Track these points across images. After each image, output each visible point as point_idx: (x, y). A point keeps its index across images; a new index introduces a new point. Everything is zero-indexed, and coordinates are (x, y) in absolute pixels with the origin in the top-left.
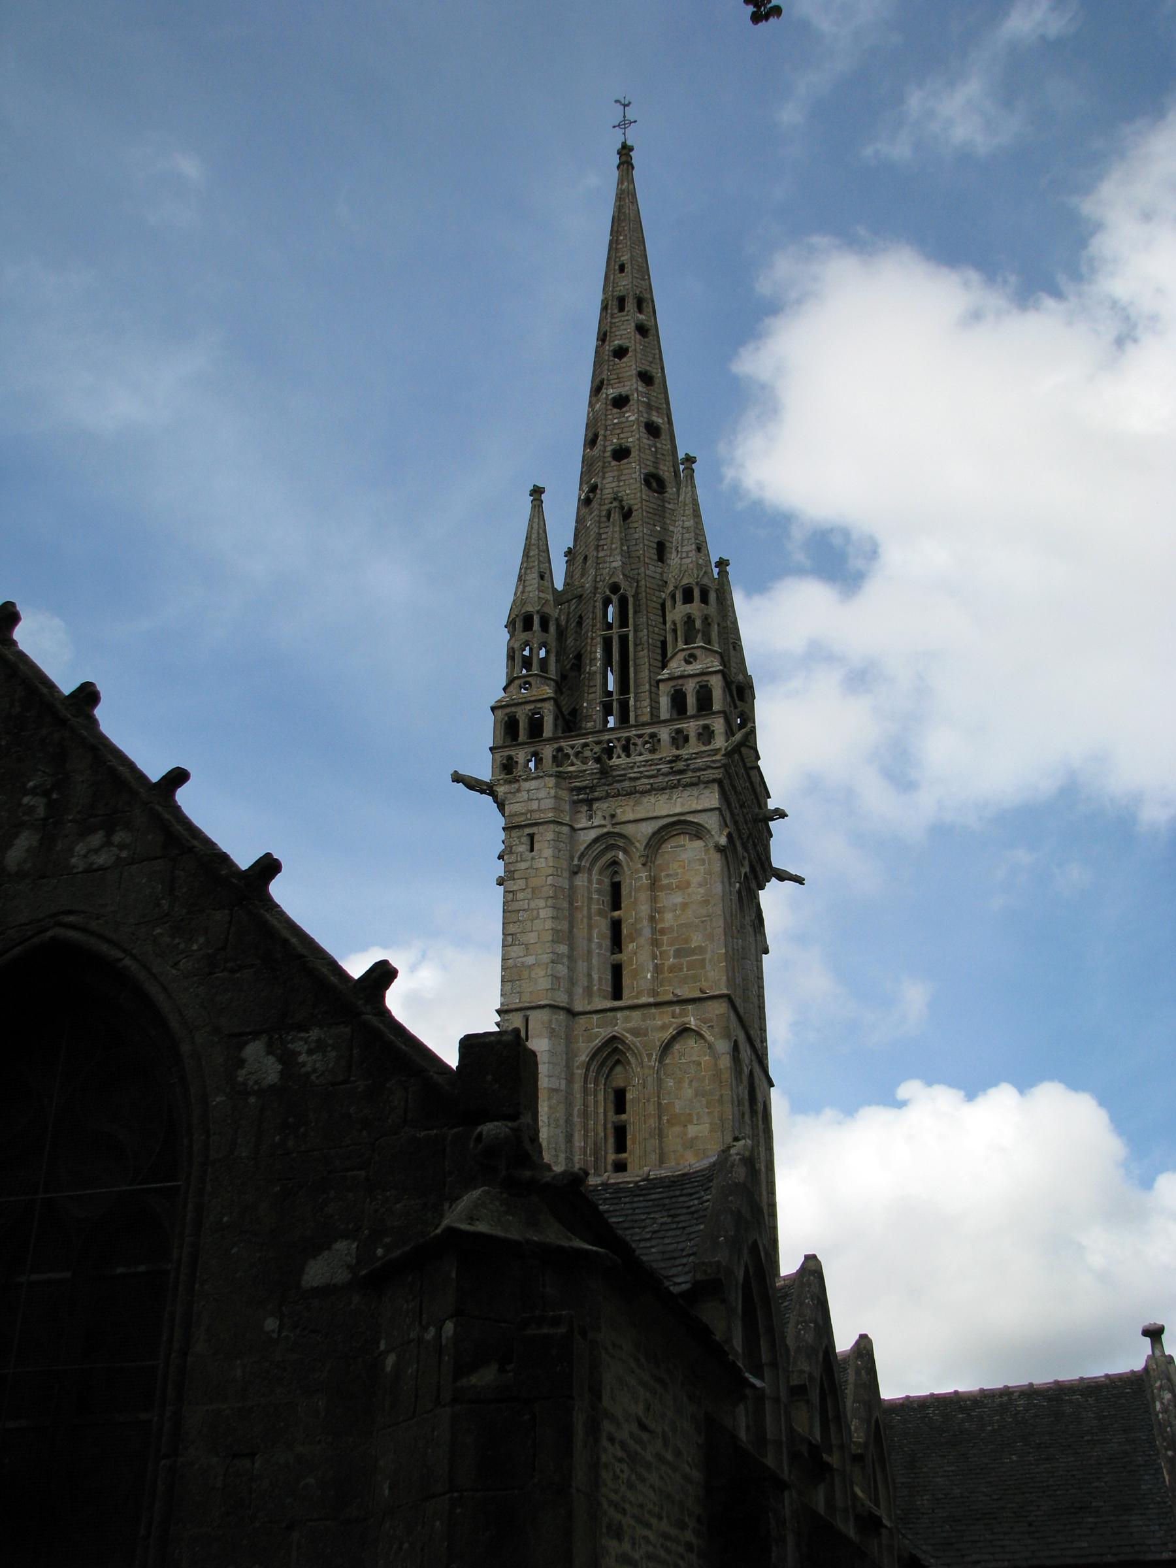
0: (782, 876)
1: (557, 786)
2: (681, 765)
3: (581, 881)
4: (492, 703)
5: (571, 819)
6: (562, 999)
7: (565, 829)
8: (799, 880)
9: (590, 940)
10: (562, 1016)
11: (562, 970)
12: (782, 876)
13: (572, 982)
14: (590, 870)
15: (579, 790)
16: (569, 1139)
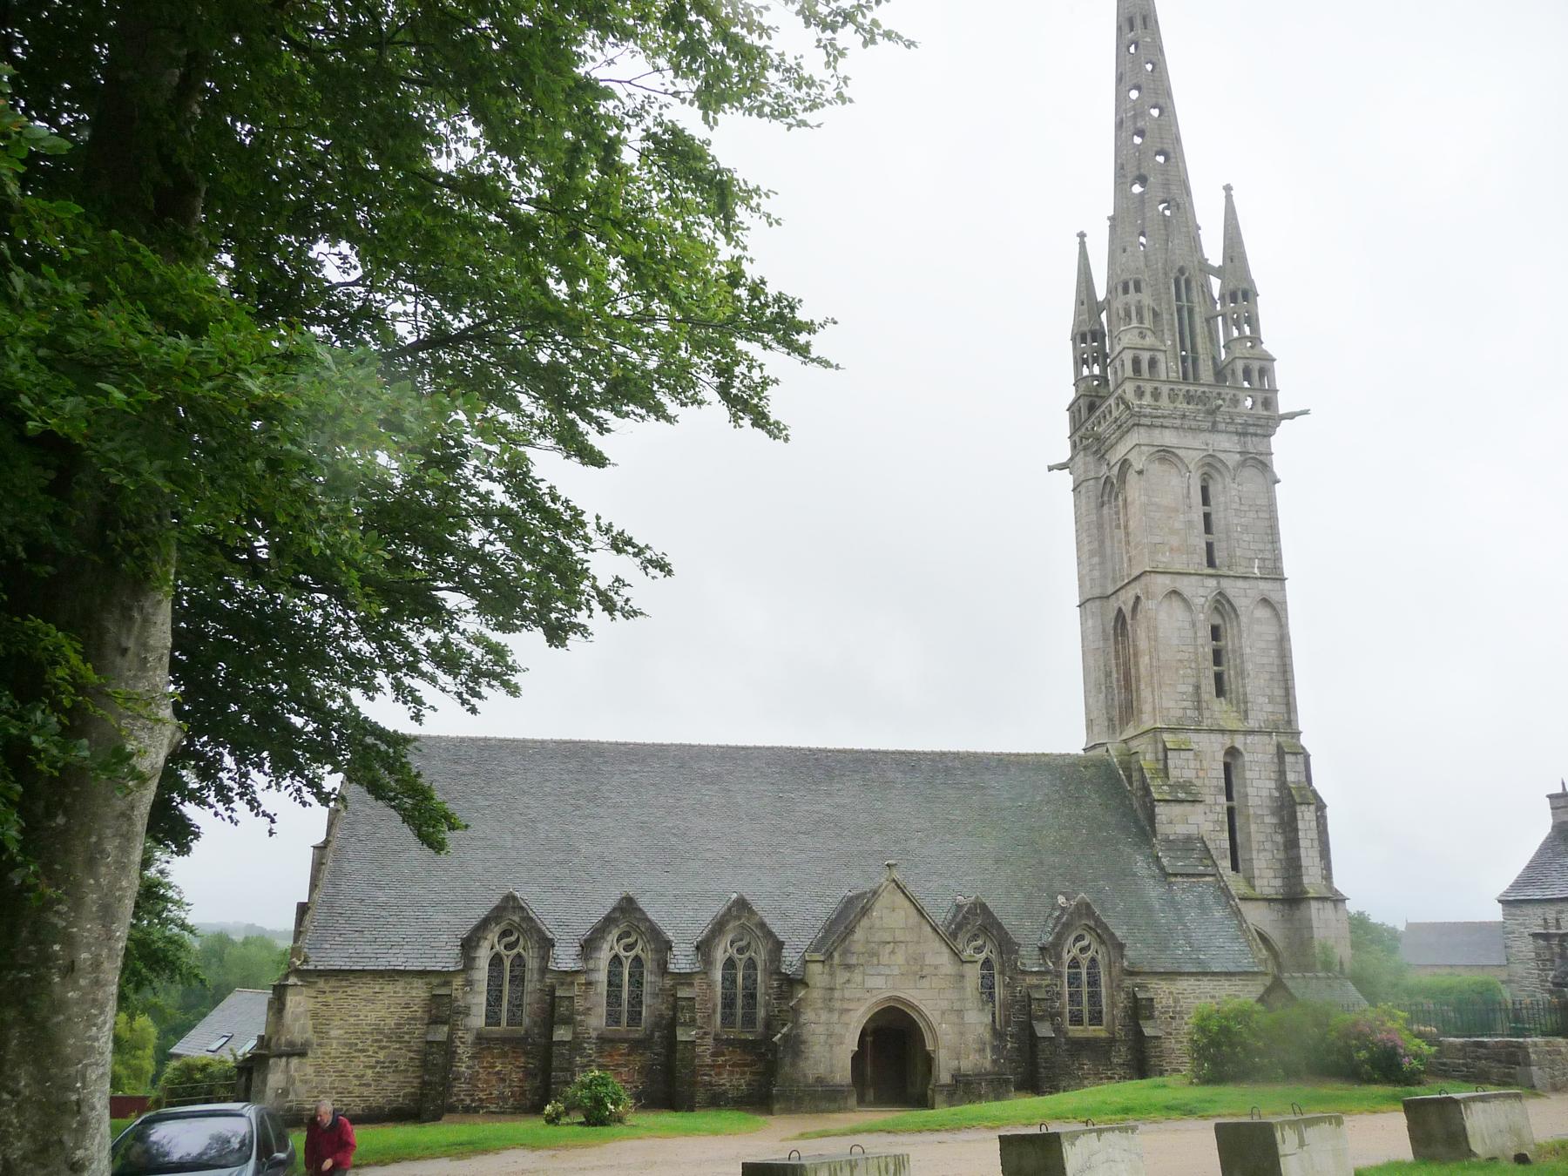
0: (1291, 416)
1: (1085, 456)
2: (1119, 423)
3: (1106, 510)
4: (1067, 407)
5: (1097, 472)
6: (1097, 592)
7: (1092, 482)
8: (1305, 412)
9: (1113, 546)
10: (1098, 603)
11: (1096, 574)
12: (1291, 416)
13: (1104, 577)
14: (1109, 502)
15: (1096, 452)
16: (1108, 675)
